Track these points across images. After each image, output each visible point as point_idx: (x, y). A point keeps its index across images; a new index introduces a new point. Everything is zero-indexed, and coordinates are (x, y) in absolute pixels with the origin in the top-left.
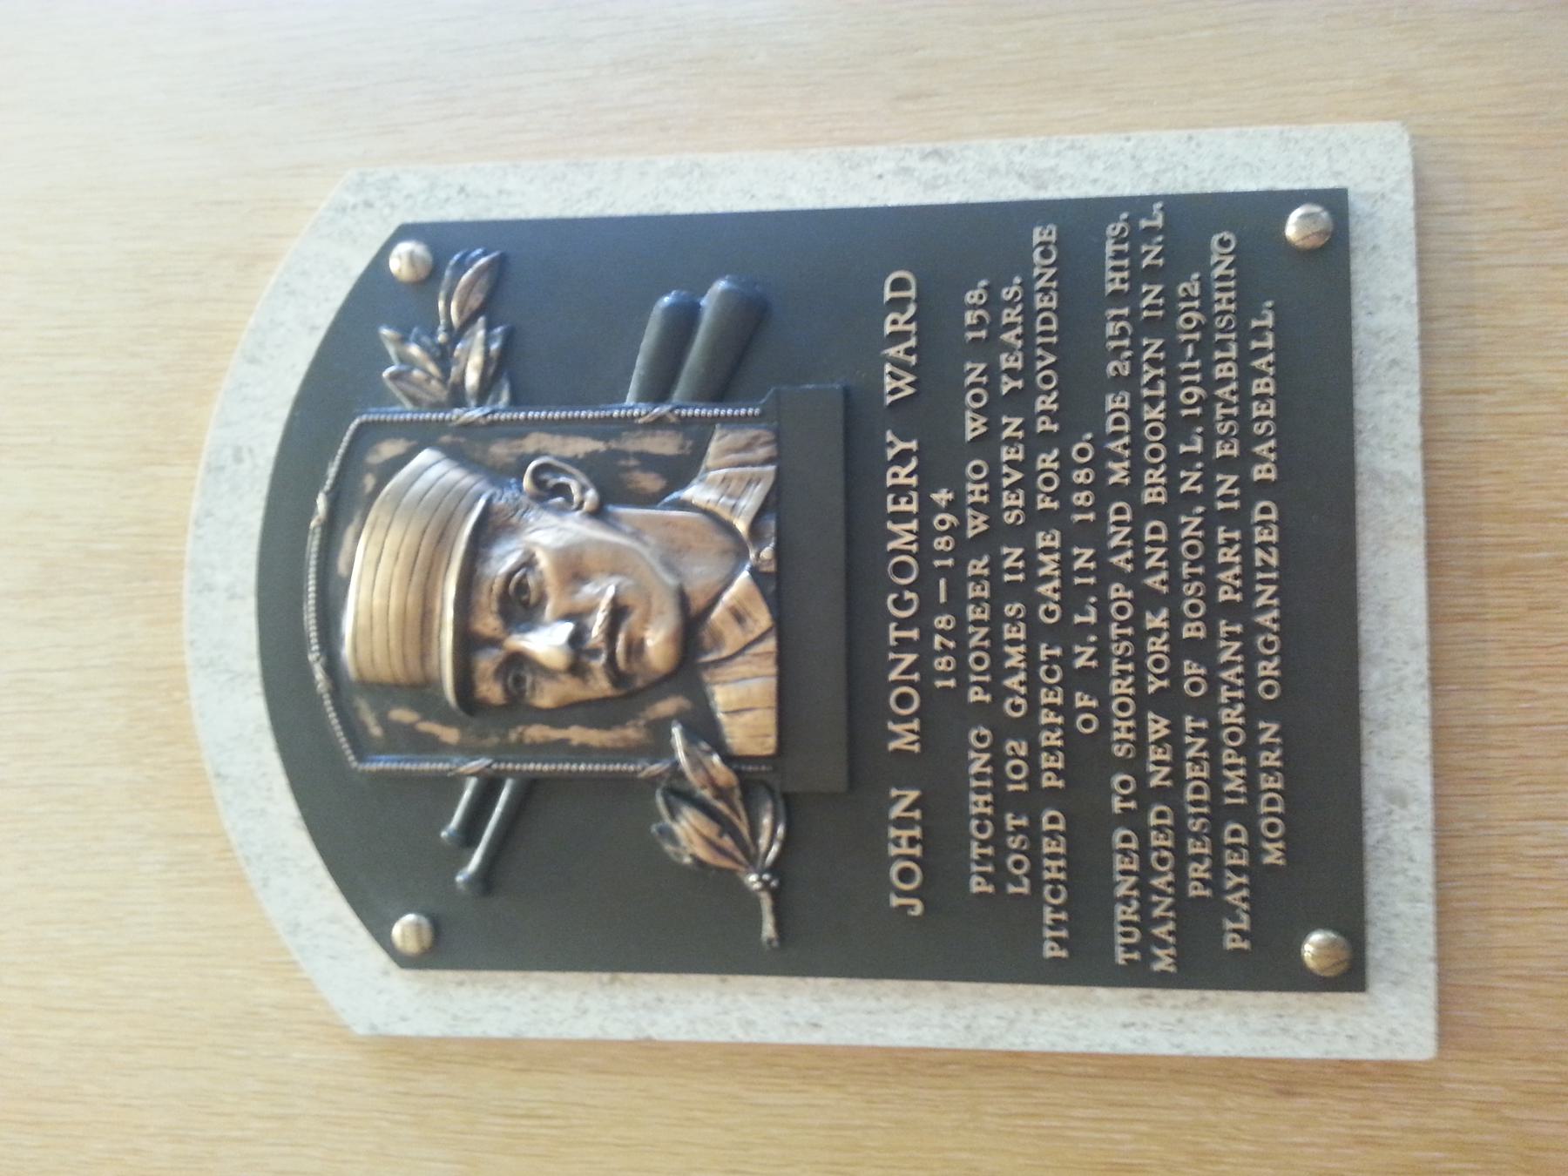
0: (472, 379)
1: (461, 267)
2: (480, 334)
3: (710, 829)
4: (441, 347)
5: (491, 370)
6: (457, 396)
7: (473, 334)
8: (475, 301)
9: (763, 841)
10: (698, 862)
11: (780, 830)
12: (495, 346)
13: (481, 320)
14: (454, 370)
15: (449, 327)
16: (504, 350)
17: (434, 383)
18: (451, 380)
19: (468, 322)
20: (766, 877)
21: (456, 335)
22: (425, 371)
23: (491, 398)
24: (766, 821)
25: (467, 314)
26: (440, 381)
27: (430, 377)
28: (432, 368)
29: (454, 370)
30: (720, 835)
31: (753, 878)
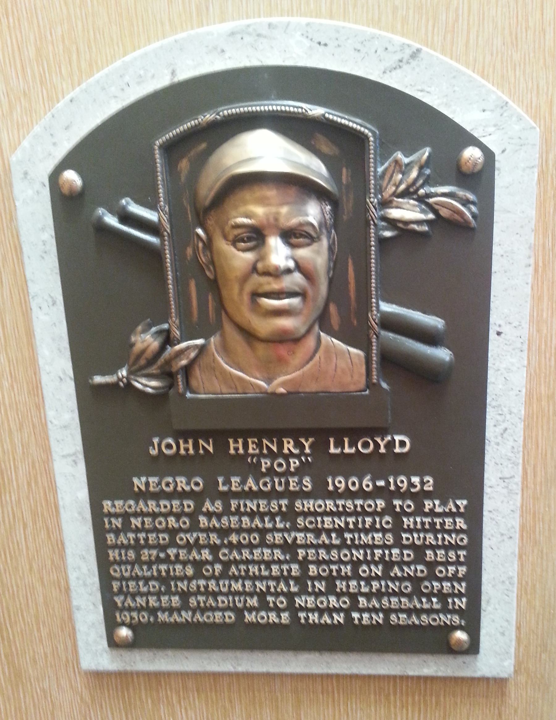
0: (394, 213)
1: (466, 202)
2: (422, 216)
3: (149, 354)
5: (400, 225)
6: (385, 204)
7: (422, 211)
8: (444, 212)
9: (144, 381)
11: (149, 390)
13: (431, 216)
14: (400, 200)
16: (414, 232)
17: (394, 188)
18: (395, 199)
19: (432, 208)
21: (421, 200)
22: (401, 182)
23: (383, 223)
24: (154, 383)
25: (437, 207)
26: (395, 192)
27: (397, 187)
28: (403, 187)
30: (147, 359)
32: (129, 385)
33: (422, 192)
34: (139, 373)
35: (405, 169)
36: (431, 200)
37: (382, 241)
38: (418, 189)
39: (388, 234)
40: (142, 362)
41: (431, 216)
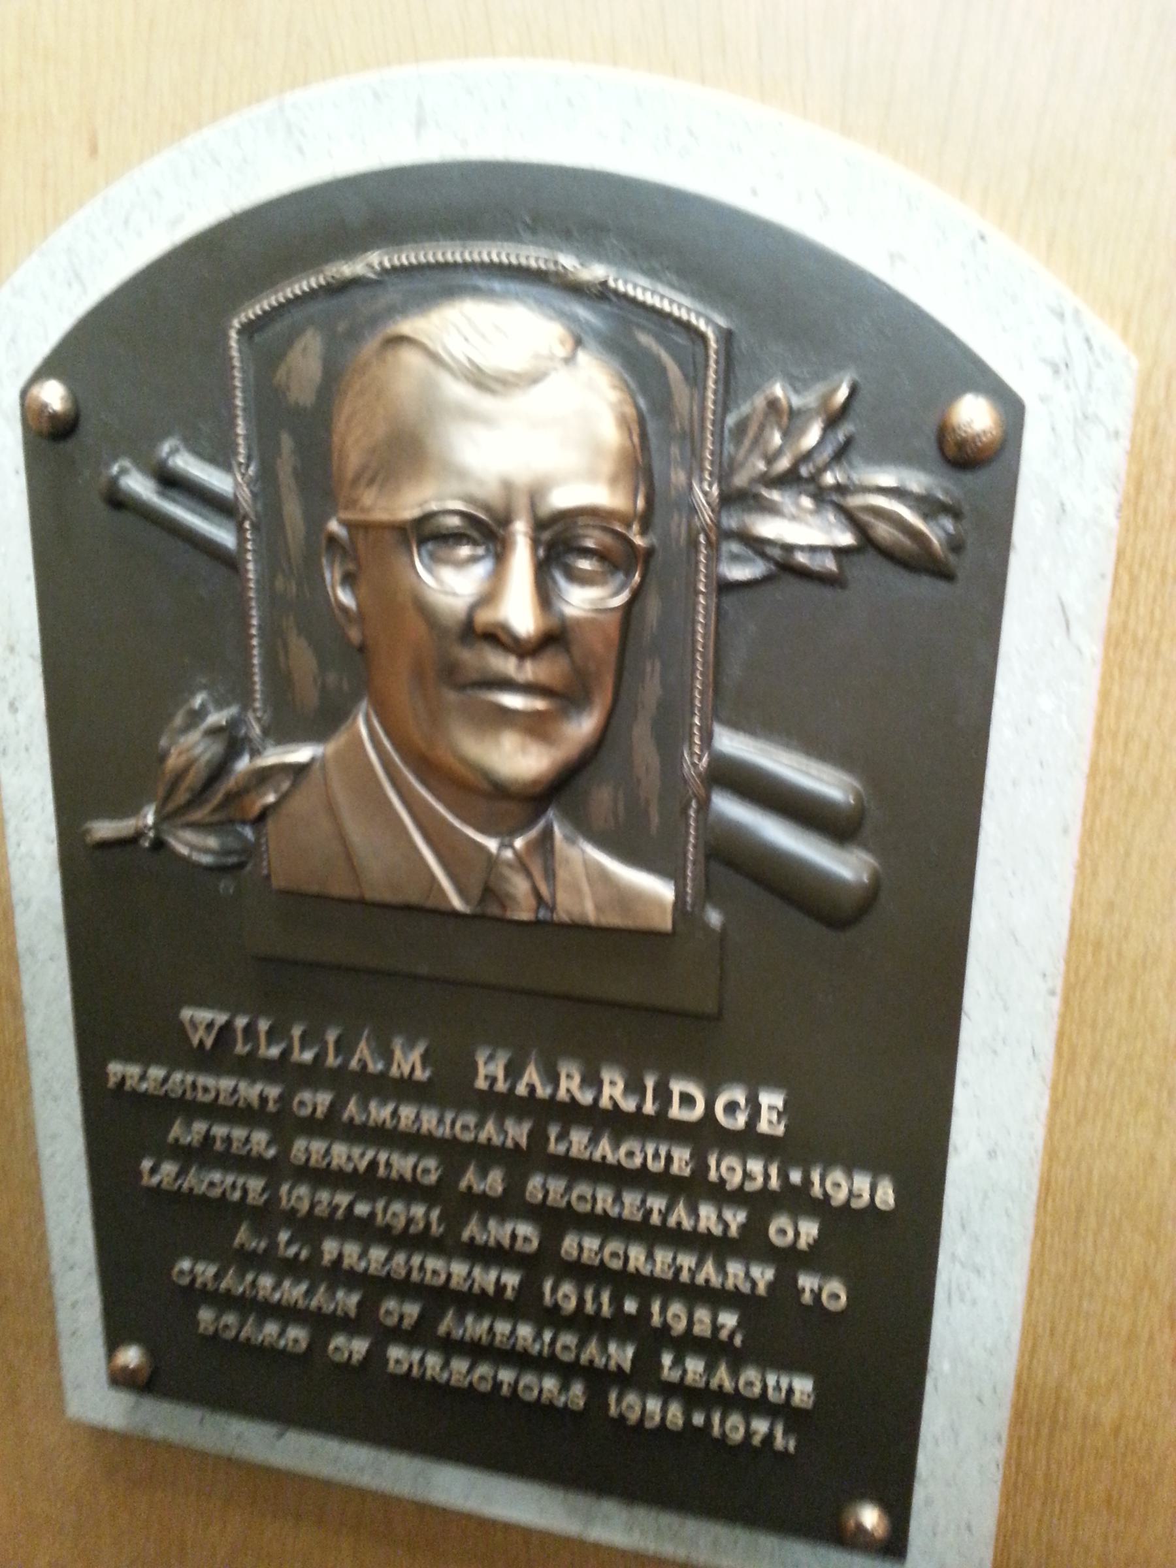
4: (814, 479)
6: (736, 498)
10: (163, 757)
12: (801, 558)
15: (840, 489)
16: (804, 573)
17: (761, 466)
19: (851, 518)
20: (151, 834)
22: (779, 453)
27: (770, 460)
28: (784, 464)
29: (775, 495)
31: (150, 820)
32: (159, 844)
33: (829, 479)
34: (180, 821)
35: (792, 421)
36: (855, 501)
37: (726, 587)
38: (821, 471)
39: (739, 573)
40: (181, 797)
41: (846, 539)
